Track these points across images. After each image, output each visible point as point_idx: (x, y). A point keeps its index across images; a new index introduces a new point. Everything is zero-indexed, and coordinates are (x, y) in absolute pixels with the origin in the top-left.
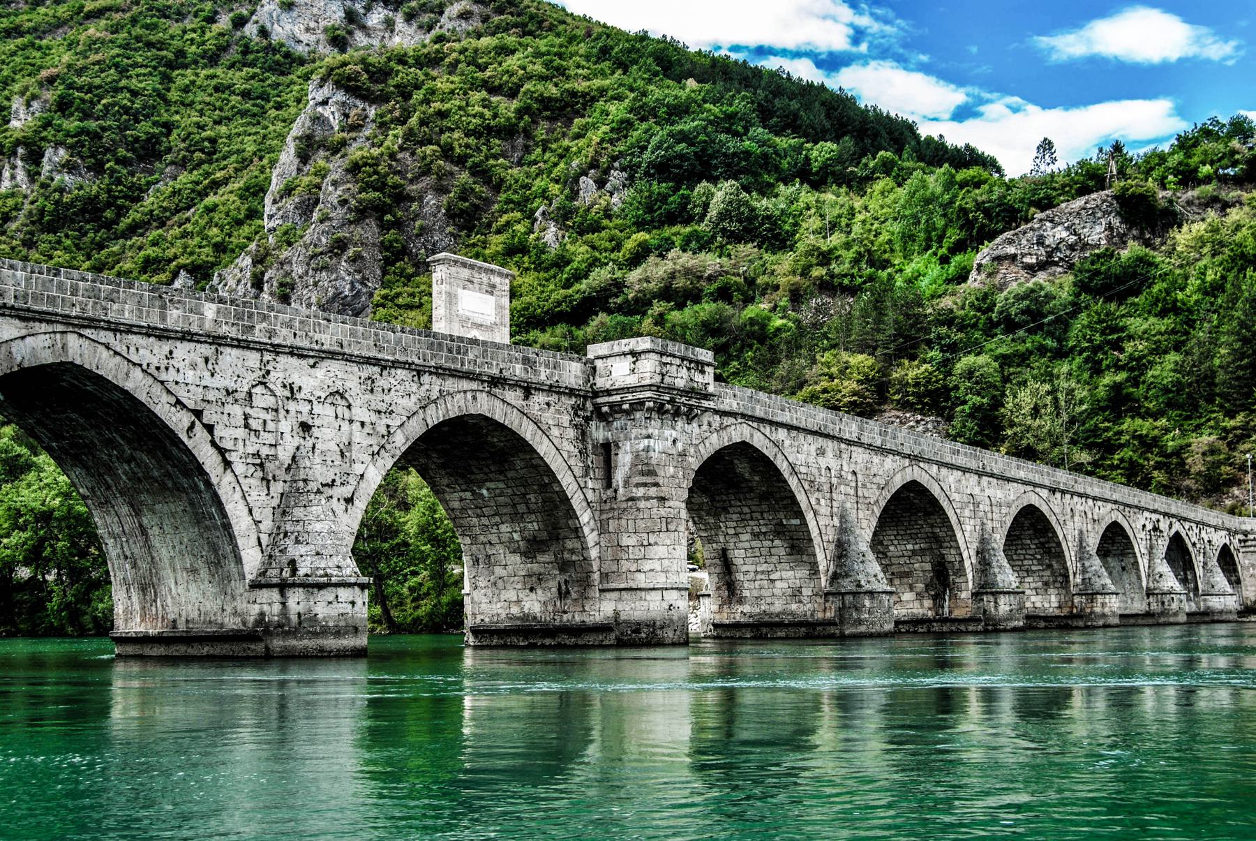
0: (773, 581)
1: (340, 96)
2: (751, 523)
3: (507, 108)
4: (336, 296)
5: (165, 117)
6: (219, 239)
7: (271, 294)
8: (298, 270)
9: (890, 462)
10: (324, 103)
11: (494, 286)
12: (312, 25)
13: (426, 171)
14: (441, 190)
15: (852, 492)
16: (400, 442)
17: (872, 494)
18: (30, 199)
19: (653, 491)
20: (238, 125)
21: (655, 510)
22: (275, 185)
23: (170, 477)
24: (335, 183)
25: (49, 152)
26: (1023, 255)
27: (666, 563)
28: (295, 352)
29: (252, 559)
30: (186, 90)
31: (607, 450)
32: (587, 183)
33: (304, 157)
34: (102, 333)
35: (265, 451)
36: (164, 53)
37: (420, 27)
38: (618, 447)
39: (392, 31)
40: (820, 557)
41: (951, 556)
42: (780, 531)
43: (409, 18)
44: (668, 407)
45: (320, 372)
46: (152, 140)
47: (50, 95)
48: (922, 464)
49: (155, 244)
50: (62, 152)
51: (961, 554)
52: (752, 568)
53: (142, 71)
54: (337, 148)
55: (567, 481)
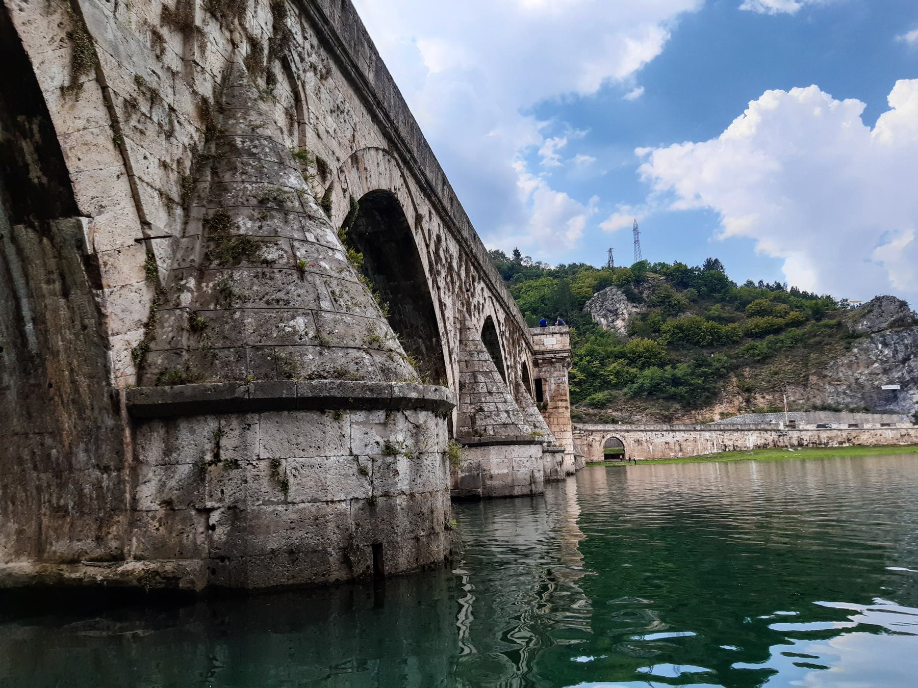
38: (545, 380)
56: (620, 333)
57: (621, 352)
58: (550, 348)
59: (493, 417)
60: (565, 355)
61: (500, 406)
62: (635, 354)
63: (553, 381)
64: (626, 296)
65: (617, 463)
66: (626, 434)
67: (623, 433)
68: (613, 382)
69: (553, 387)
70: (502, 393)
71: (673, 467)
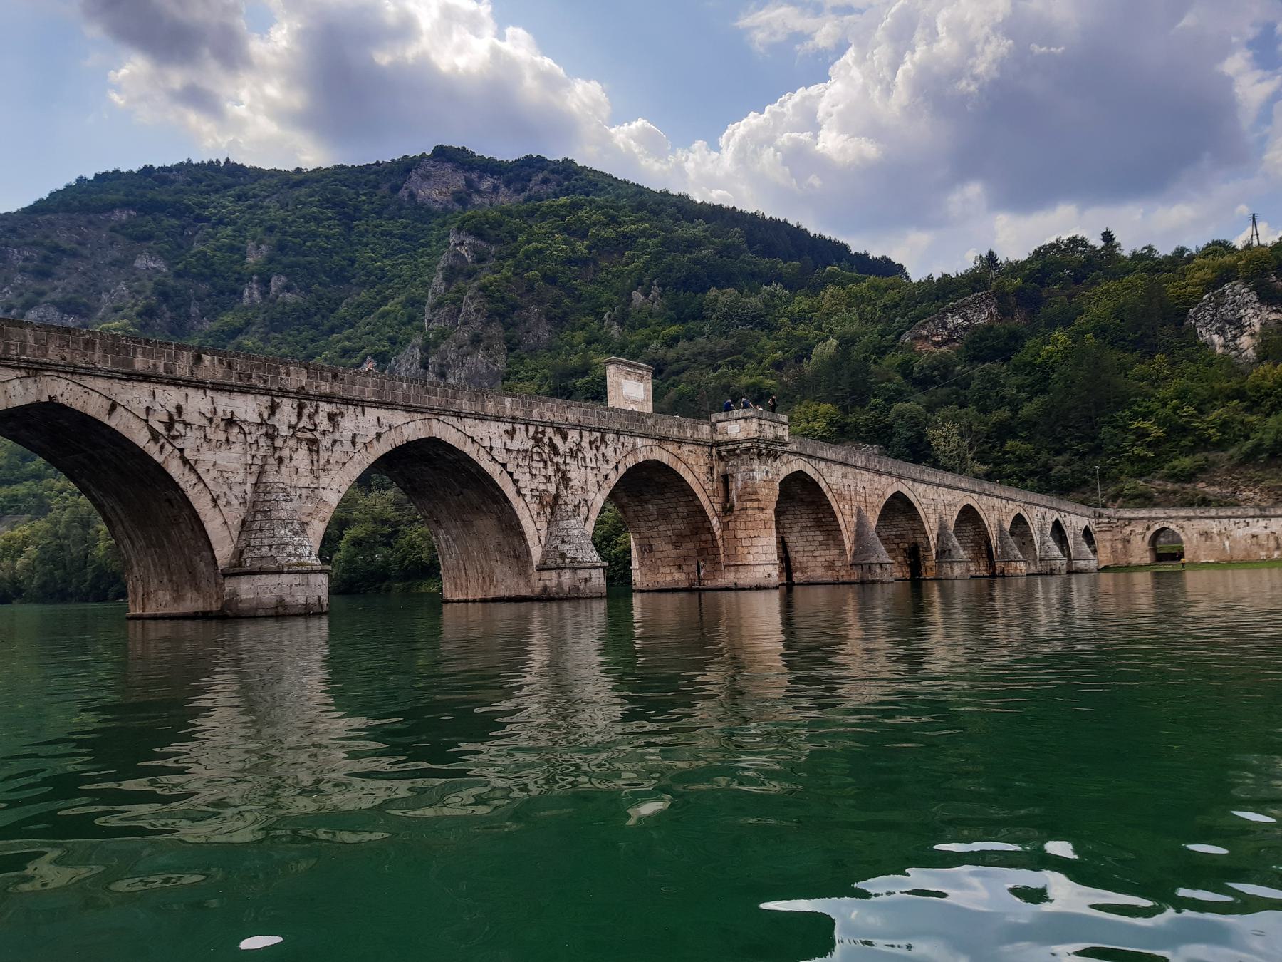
0: (816, 556)
2: (801, 521)
3: (581, 246)
7: (434, 372)
9: (885, 480)
10: (461, 244)
11: (642, 377)
12: (444, 190)
14: (540, 303)
15: (863, 500)
17: (875, 500)
18: (264, 310)
19: (755, 504)
20: (398, 259)
21: (757, 516)
22: (430, 299)
24: (471, 298)
25: (274, 279)
26: (933, 336)
27: (765, 548)
29: (536, 553)
31: (725, 479)
32: (637, 296)
33: (449, 280)
34: (451, 418)
37: (515, 191)
38: (732, 477)
39: (498, 193)
40: (846, 541)
41: (920, 538)
42: (819, 524)
43: (508, 185)
44: (764, 451)
46: (342, 269)
47: (273, 239)
48: (903, 481)
49: (349, 339)
50: (283, 279)
51: (928, 538)
52: (801, 549)
53: (332, 222)
54: (470, 275)
55: (703, 498)
56: (1246, 357)
57: (1237, 390)
58: (733, 437)
59: (256, 551)
60: (749, 445)
61: (266, 542)
62: (1259, 391)
63: (739, 477)
64: (1258, 295)
65: (1169, 566)
66: (1186, 524)
67: (1180, 522)
68: (1214, 438)
69: (740, 484)
70: (273, 529)
71: (1265, 573)
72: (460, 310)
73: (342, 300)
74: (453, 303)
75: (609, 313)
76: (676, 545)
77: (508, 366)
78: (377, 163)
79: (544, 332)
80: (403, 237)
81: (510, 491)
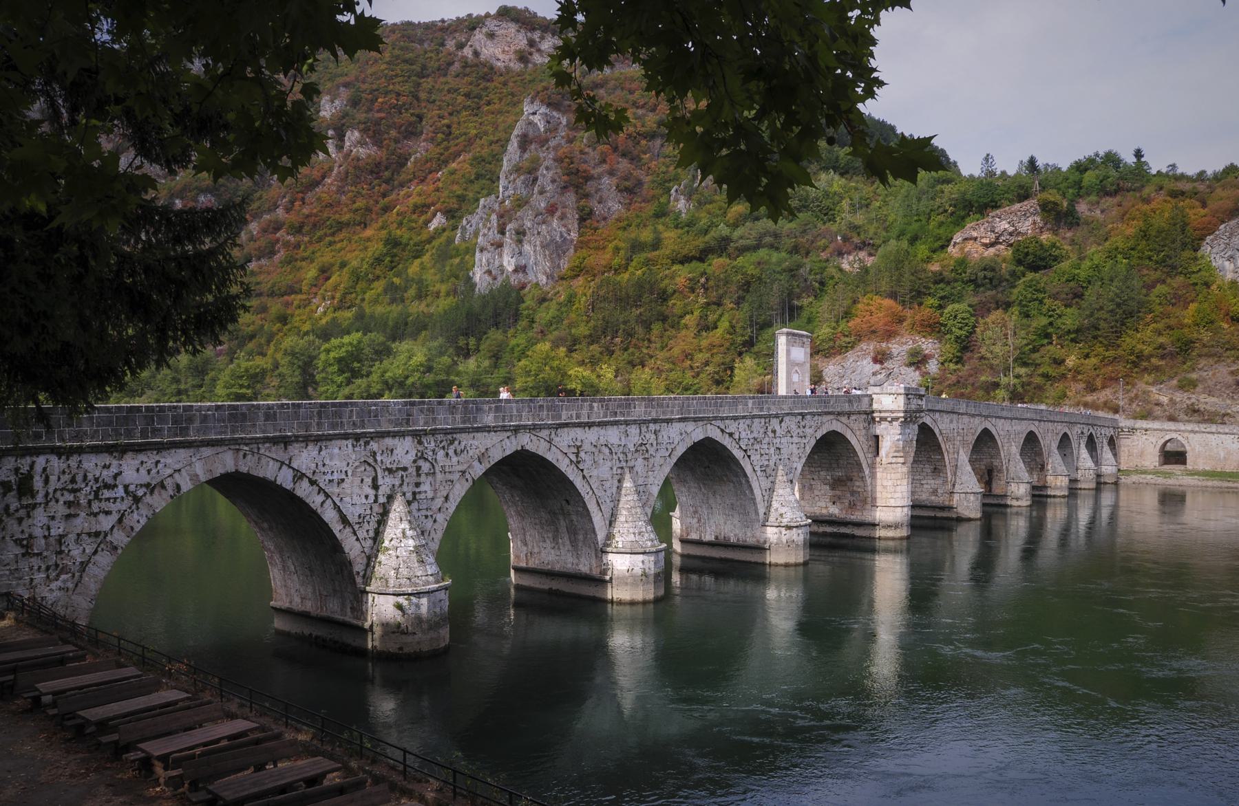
1: (543, 110)
4: (552, 240)
5: (417, 111)
6: (459, 192)
8: (529, 224)
10: (534, 113)
12: (506, 49)
13: (604, 161)
14: (611, 173)
16: (808, 450)
23: (726, 476)
25: (348, 134)
28: (776, 416)
30: (430, 92)
35: (766, 463)
36: (414, 67)
45: (783, 424)
46: (410, 124)
50: (357, 134)
54: (543, 142)
72: (536, 179)
73: (410, 155)
74: (530, 173)
75: (676, 187)
76: (833, 489)
77: (581, 235)
78: (443, 21)
79: (615, 205)
80: (467, 95)
81: (748, 470)
